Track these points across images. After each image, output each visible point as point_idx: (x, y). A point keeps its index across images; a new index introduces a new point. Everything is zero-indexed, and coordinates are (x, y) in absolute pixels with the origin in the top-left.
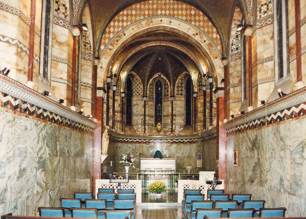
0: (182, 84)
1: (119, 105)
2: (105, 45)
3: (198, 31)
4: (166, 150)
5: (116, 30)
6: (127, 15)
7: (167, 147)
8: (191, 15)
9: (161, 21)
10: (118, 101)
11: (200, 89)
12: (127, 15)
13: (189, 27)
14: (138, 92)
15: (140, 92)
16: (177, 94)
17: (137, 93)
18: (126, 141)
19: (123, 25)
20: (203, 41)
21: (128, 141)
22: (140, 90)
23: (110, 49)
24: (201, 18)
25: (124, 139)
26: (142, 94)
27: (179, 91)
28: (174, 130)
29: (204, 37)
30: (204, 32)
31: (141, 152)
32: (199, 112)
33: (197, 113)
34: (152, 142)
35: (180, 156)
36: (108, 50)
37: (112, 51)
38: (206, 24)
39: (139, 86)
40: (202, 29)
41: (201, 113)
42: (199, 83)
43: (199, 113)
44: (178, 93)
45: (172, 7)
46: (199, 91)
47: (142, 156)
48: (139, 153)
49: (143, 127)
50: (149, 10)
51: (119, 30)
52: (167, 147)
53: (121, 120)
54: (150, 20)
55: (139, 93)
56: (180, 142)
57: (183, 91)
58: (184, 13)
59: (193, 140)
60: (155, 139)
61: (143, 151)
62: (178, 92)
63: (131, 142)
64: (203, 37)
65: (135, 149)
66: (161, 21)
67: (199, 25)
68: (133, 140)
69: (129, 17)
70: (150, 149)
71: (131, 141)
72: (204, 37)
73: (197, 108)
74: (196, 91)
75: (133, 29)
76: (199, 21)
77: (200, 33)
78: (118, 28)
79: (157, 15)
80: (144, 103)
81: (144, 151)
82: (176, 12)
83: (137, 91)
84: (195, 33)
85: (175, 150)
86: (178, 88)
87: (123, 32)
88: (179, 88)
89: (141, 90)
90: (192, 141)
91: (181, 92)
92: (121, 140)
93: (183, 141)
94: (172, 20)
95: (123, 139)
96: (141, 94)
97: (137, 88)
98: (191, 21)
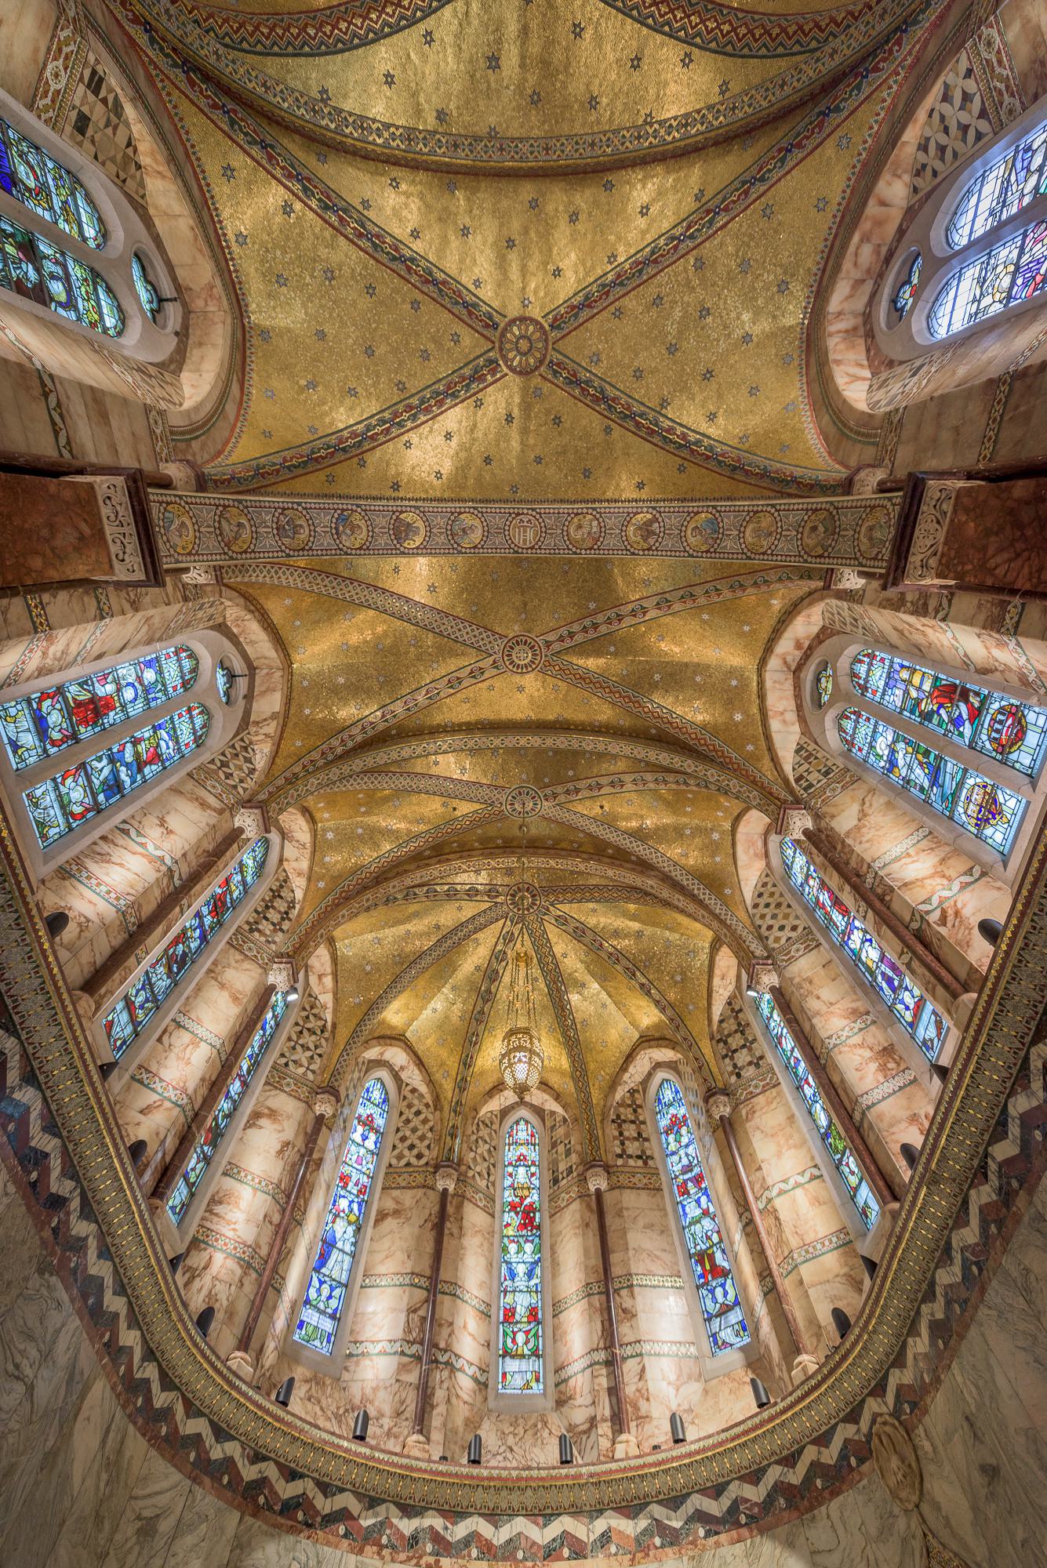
0: (635, 1111)
1: (286, 1144)
10: (286, 1124)
11: (735, 1066)
14: (412, 1147)
15: (426, 1142)
16: (620, 1156)
17: (406, 1152)
21: (262, 1482)
22: (422, 1138)
25: (233, 1449)
26: (435, 1153)
27: (628, 1139)
28: (636, 1408)
32: (783, 1186)
33: (770, 1200)
39: (422, 1117)
41: (799, 1192)
42: (721, 1045)
43: (781, 1193)
44: (624, 1151)
46: (739, 1075)
49: (413, 1377)
55: (415, 1152)
57: (647, 1140)
60: (491, 1500)
62: (623, 1144)
63: (289, 1507)
71: (287, 1490)
73: (760, 1168)
74: (720, 1085)
80: (437, 1208)
83: (408, 1143)
86: (620, 1126)
88: (625, 1126)
89: (429, 1135)
91: (636, 1144)
93: (725, 1502)
95: (221, 1433)
96: (426, 1152)
97: (411, 1125)
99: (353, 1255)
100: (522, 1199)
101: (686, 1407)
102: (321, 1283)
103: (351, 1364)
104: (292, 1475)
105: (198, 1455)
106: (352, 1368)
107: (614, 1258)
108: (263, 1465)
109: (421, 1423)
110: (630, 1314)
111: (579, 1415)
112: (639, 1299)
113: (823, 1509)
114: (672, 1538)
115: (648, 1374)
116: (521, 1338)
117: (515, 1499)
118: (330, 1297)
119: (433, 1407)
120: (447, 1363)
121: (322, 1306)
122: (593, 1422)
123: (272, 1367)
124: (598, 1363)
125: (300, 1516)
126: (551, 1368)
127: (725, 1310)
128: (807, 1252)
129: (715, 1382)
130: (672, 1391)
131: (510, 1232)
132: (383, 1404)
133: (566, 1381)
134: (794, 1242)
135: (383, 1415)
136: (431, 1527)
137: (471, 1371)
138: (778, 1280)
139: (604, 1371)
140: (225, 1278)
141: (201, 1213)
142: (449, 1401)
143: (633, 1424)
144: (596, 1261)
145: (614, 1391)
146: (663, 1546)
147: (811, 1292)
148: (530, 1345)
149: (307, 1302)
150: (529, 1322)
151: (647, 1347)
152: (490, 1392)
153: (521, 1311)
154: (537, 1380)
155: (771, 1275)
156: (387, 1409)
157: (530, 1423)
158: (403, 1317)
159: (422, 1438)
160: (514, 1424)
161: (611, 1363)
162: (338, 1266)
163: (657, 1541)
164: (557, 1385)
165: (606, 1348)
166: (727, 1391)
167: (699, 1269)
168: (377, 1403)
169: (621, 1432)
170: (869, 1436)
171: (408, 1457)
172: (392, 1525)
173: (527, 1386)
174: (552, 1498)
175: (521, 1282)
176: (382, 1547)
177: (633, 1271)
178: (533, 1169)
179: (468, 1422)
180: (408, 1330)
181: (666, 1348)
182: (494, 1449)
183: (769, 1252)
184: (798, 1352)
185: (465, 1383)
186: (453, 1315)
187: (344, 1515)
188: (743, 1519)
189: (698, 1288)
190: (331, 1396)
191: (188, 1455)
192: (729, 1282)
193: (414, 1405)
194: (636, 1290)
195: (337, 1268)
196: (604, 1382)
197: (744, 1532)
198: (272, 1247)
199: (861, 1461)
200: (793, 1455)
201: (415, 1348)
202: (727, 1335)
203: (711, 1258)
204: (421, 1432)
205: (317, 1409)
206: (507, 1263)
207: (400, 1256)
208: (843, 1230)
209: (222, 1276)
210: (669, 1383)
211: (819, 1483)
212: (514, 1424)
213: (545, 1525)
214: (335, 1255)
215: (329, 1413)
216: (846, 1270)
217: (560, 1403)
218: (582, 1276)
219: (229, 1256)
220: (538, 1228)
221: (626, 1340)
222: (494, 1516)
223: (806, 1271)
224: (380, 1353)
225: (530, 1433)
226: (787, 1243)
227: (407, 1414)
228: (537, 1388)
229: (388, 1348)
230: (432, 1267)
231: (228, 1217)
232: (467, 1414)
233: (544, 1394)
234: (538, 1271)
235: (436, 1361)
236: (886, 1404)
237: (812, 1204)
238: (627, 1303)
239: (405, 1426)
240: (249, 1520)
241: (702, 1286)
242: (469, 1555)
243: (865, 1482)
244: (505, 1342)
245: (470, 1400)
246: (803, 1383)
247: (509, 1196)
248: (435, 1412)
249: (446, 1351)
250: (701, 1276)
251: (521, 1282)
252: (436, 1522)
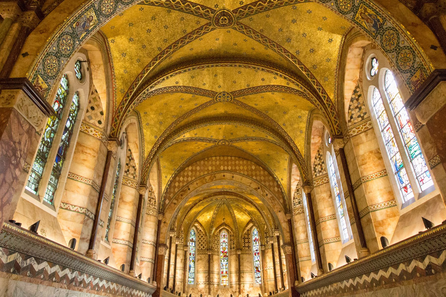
2: (170, 199)
3: (259, 185)
5: (181, 184)
6: (192, 171)
8: (252, 170)
9: (224, 176)
12: (192, 171)
13: (250, 181)
19: (187, 180)
20: (265, 194)
23: (175, 204)
24: (262, 173)
28: (242, 291)
29: (266, 191)
30: (265, 186)
36: (173, 205)
37: (176, 206)
38: (267, 178)
40: (263, 183)
45: (233, 163)
49: (207, 287)
50: (212, 165)
51: (184, 185)
53: (183, 278)
54: (213, 175)
58: (245, 168)
64: (264, 191)
66: (224, 176)
67: (260, 179)
69: (194, 173)
72: (266, 191)
75: (197, 184)
76: (260, 176)
77: (261, 187)
78: (183, 183)
79: (221, 171)
82: (237, 168)
84: (257, 187)
87: (188, 186)
94: (235, 175)
98: (252, 175)
100: (224, 250)
107: (241, 267)
109: (209, 293)
110: (243, 277)
111: (234, 290)
112: (244, 275)
115: (245, 287)
122: (236, 292)
131: (222, 257)
133: (232, 284)
137: (216, 284)
143: (242, 293)
144: (238, 267)
145: (239, 288)
147: (269, 286)
151: (245, 283)
158: (205, 278)
161: (239, 285)
175: (224, 267)
178: (226, 244)
184: (265, 292)
185: (216, 286)
196: (238, 287)
207: (203, 268)
220: (227, 257)
223: (269, 282)
238: (243, 275)
239: (207, 294)
247: (221, 250)
251: (224, 267)
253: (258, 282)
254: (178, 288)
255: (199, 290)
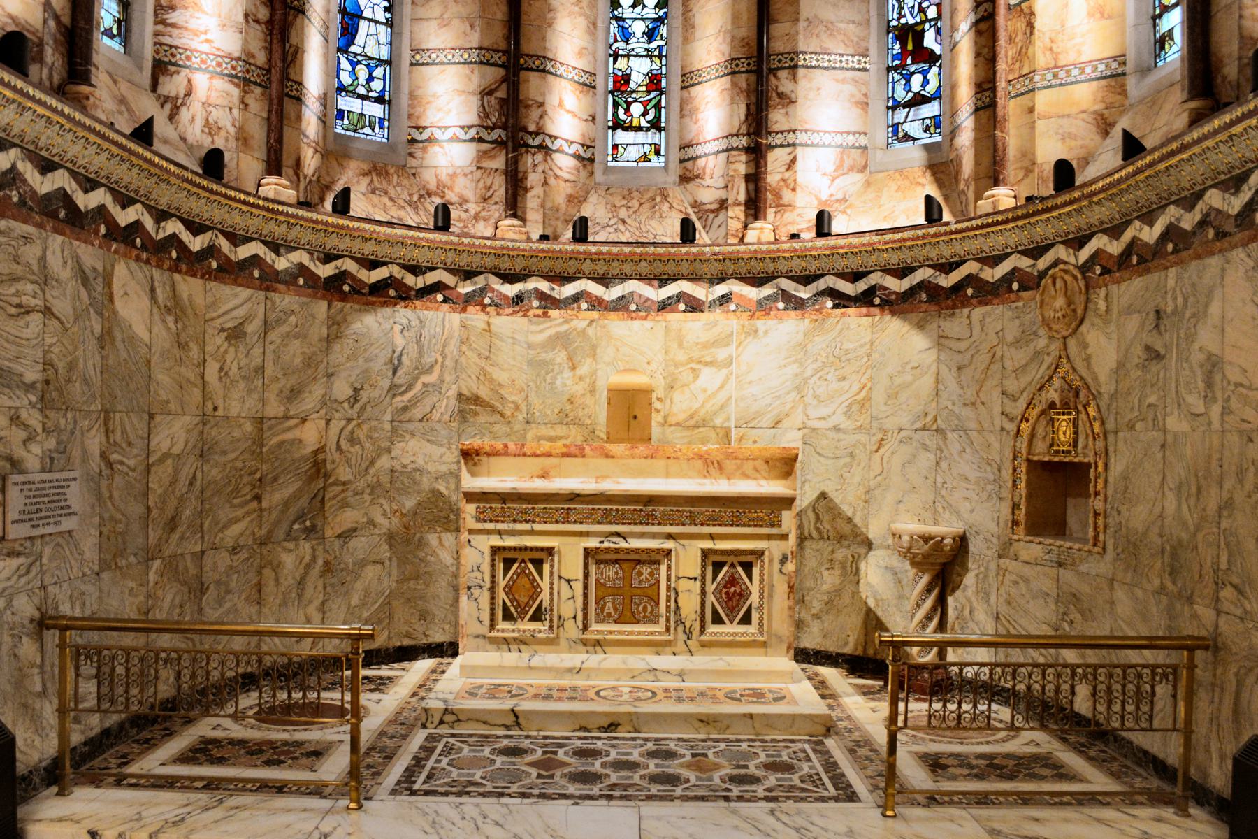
4: (706, 373)
7: (716, 343)
18: (325, 271)
21: (342, 276)
28: (778, 195)
31: (471, 385)
34: (576, 298)
35: (836, 429)
47: (483, 418)
48: (452, 393)
49: (499, 162)
52: (716, 343)
56: (831, 293)
59: (970, 268)
60: (601, 269)
61: (492, 381)
63: (378, 289)
65: (421, 354)
68: (397, 272)
70: (560, 356)
81: (501, 376)
85: (794, 369)
90: (970, 279)
92: (255, 260)
93: (862, 286)
99: (390, 24)
101: (840, 196)
102: (354, 64)
103: (416, 150)
104: (373, 265)
105: (262, 271)
106: (419, 154)
108: (339, 262)
109: (514, 206)
110: (787, 100)
111: (708, 196)
113: (966, 311)
114: (797, 304)
115: (799, 164)
116: (637, 109)
117: (628, 268)
118: (370, 79)
119: (526, 190)
120: (542, 147)
121: (361, 91)
122: (723, 204)
123: (318, 169)
124: (737, 149)
125: (392, 293)
126: (675, 144)
127: (919, 100)
128: (1055, 76)
129: (882, 175)
130: (826, 181)
132: (464, 189)
133: (694, 159)
134: (1042, 59)
135: (467, 201)
136: (536, 290)
137: (573, 149)
138: (1000, 102)
139: (743, 158)
140: (219, 102)
141: (150, 27)
142: (545, 183)
143: (771, 213)
144: (747, 30)
145: (755, 179)
146: (785, 309)
147: (1040, 125)
148: (650, 117)
149: (341, 89)
150: (649, 92)
151: (802, 138)
152: (598, 167)
153: (637, 79)
154: (658, 153)
155: (994, 90)
156: (470, 194)
157: (647, 197)
158: (475, 101)
159: (517, 222)
160: (628, 195)
161: (756, 153)
162: (372, 40)
163: (781, 305)
164: (682, 161)
165: (748, 134)
166: (894, 187)
167: (897, 46)
168: (457, 189)
169: (756, 218)
170: (1043, 274)
171: (503, 239)
172: (493, 290)
173: (645, 158)
174: (671, 268)
176: (484, 306)
177: (801, 48)
179: (570, 199)
180: (484, 114)
181: (827, 139)
182: (604, 221)
183: (1002, 66)
184: (996, 182)
185: (564, 163)
186: (543, 94)
187: (438, 287)
188: (877, 301)
189: (889, 69)
190: (398, 185)
191: (251, 274)
192: (935, 70)
193: (502, 191)
194: (801, 72)
195: (372, 42)
196: (742, 168)
197: (876, 311)
198: (269, 50)
199: (1023, 288)
200: (951, 264)
201: (495, 134)
202: (914, 129)
203: (919, 36)
204: (515, 216)
205: (386, 200)
206: (618, 19)
208: (1121, 59)
209: (213, 100)
210: (825, 174)
211: (970, 291)
212: (628, 195)
213: (660, 287)
214: (363, 26)
215: (401, 202)
216: (1099, 107)
217: (685, 179)
218: (726, 48)
219: (213, 75)
221: (776, 128)
222: (604, 280)
224: (451, 140)
225: (646, 206)
226: (1032, 60)
227: (495, 199)
228: (656, 162)
229: (461, 134)
230: (508, 39)
231: (190, 26)
232: (569, 191)
233: (666, 168)
234: (664, 30)
235: (527, 146)
236: (1076, 257)
237: (1090, 15)
239: (496, 210)
240: (339, 305)
241: (895, 68)
242: (579, 308)
243: (1020, 304)
244: (615, 113)
245: (572, 178)
246: (988, 215)
248: (529, 195)
249: (537, 134)
250: (895, 57)
251: (638, 43)
252: (544, 286)
253: (907, 137)
254: (211, 128)
255: (432, 186)
